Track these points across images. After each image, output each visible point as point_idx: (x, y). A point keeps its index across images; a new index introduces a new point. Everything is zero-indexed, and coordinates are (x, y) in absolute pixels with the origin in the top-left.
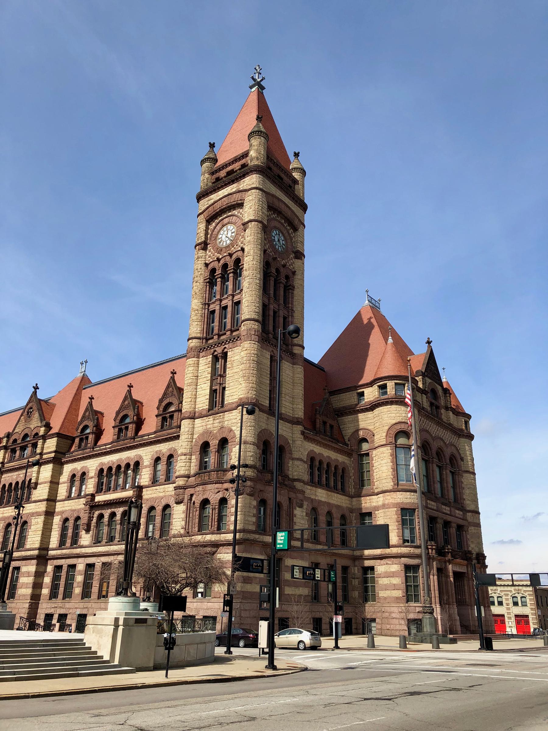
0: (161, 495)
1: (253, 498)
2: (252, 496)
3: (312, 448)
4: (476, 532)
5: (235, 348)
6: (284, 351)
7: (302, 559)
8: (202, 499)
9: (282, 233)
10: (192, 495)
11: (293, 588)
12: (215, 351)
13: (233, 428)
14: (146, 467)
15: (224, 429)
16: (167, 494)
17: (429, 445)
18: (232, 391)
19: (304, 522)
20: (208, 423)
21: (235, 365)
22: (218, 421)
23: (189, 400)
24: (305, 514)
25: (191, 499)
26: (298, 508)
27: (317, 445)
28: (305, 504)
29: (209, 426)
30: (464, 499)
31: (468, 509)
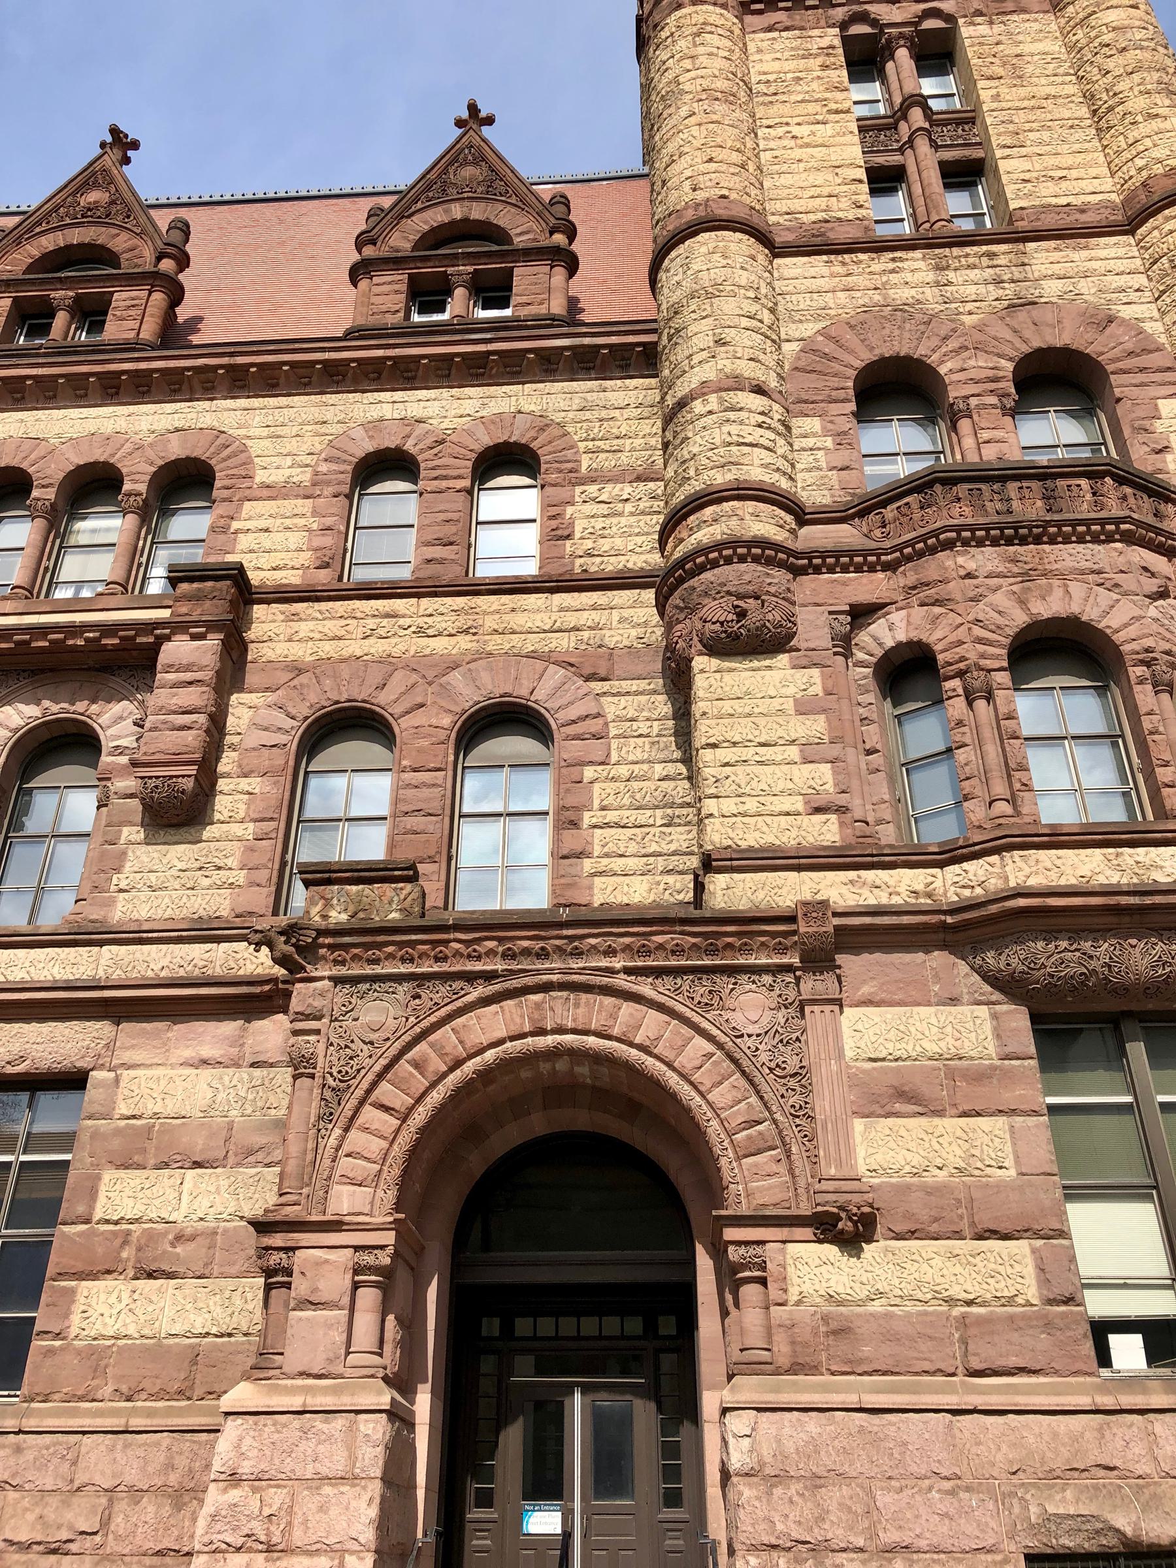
0: (440, 645)
5: (1015, 17)
8: (1020, 619)
10: (862, 614)
12: (863, 18)
13: (1126, 312)
14: (273, 492)
15: (1035, 312)
16: (495, 644)
18: (1051, 161)
20: (894, 278)
21: (1030, 69)
22: (974, 274)
23: (736, 157)
25: (845, 644)
29: (904, 294)
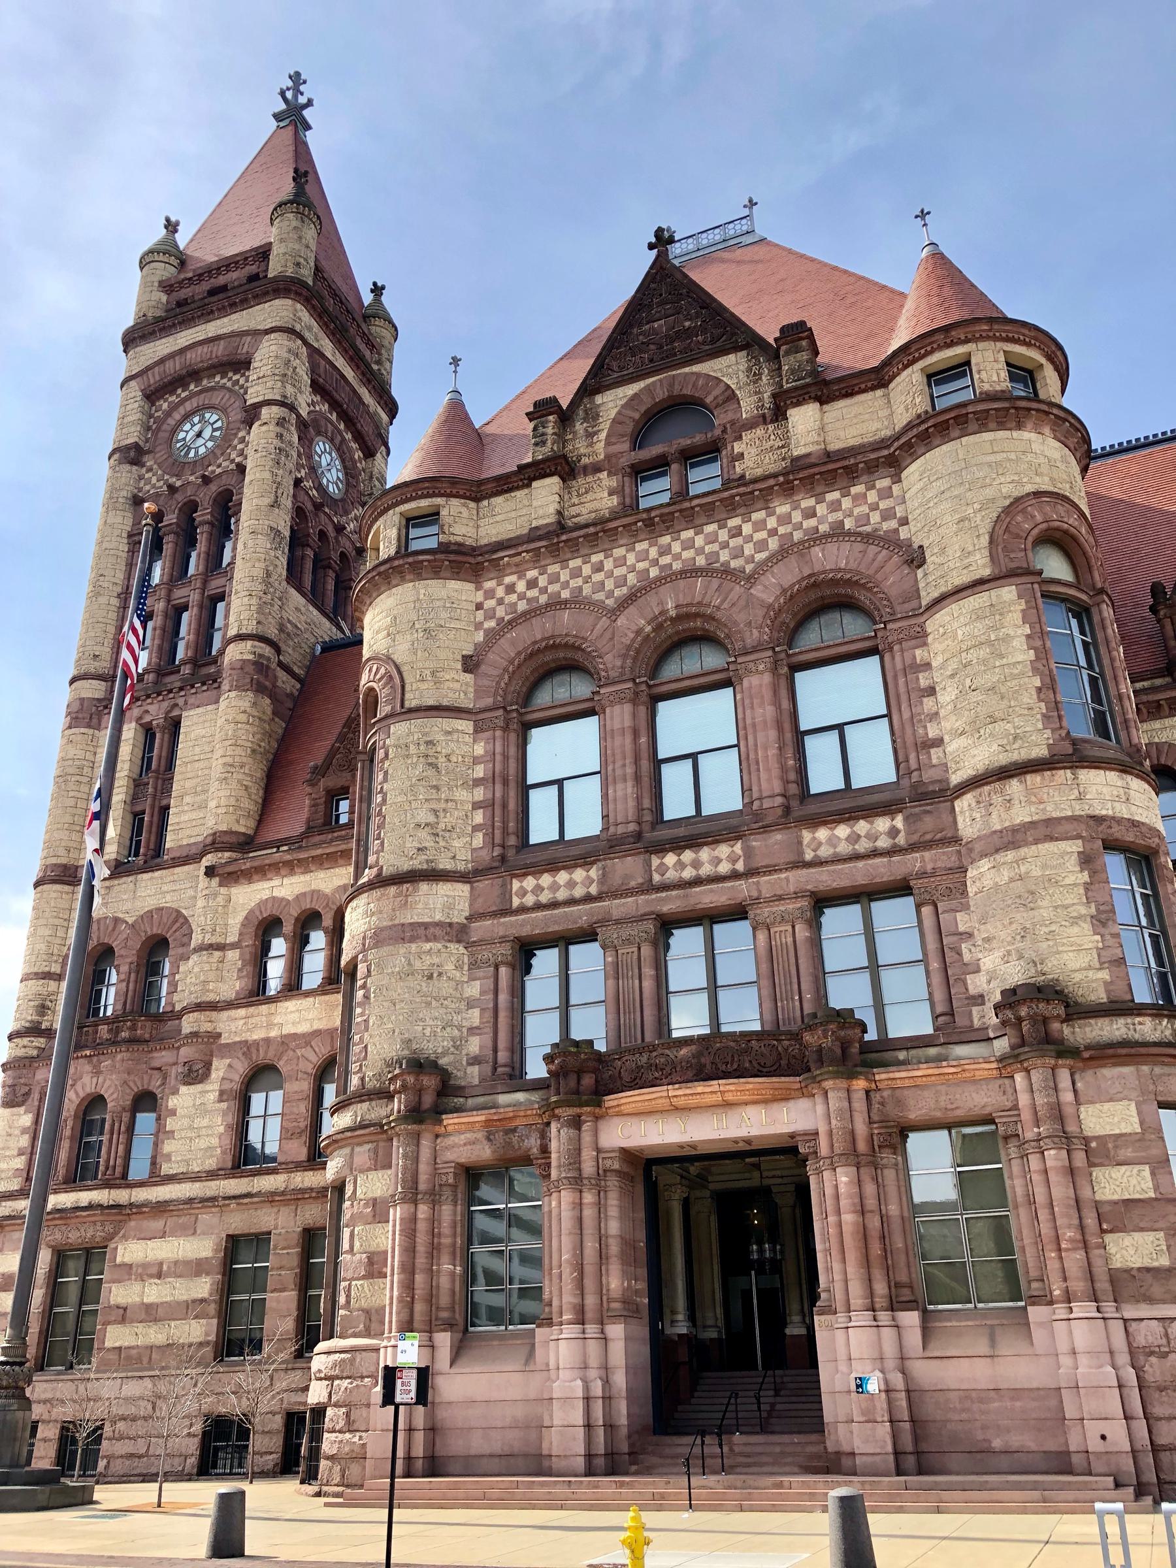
1: (22, 1110)
2: (19, 1105)
3: (265, 895)
4: (1006, 874)
6: (181, 689)
7: (191, 1231)
9: (211, 408)
11: (140, 1328)
17: (579, 648)
19: (205, 1122)
24: (213, 1096)
26: (184, 1089)
27: (292, 873)
28: (219, 1068)
30: (939, 742)
31: (955, 779)
